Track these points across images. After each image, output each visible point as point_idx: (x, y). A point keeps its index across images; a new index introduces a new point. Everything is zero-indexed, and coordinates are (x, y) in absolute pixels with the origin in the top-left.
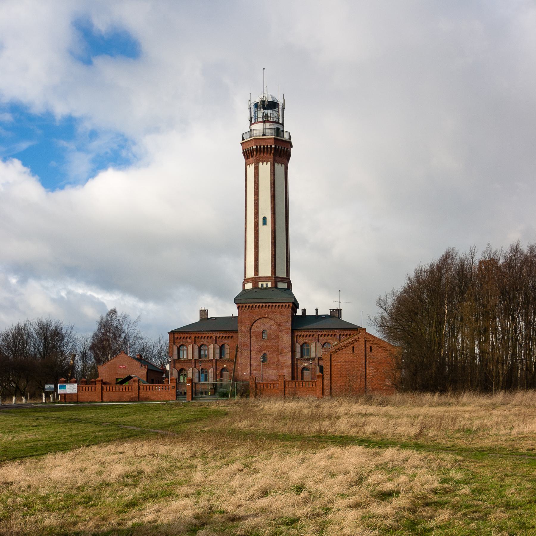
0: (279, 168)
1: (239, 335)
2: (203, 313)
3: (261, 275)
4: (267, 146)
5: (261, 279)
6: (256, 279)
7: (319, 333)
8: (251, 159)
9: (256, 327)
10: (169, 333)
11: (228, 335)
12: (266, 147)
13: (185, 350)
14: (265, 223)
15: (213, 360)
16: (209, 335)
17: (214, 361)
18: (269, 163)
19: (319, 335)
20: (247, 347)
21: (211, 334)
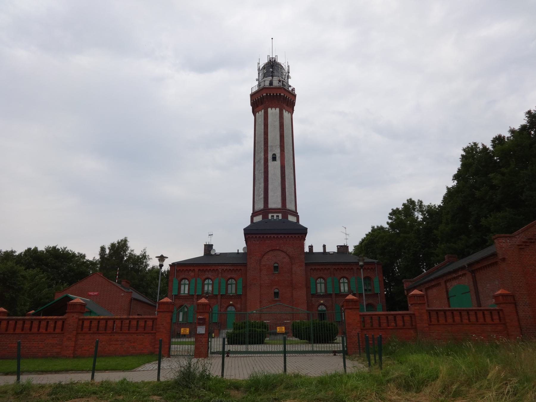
0: (286, 114)
2: (208, 248)
3: (270, 206)
4: (277, 94)
5: (270, 211)
6: (265, 211)
7: (334, 267)
8: (260, 107)
9: (267, 260)
12: (275, 94)
13: (187, 284)
14: (274, 159)
15: (218, 296)
17: (219, 297)
18: (278, 110)
19: (334, 268)
20: (256, 281)
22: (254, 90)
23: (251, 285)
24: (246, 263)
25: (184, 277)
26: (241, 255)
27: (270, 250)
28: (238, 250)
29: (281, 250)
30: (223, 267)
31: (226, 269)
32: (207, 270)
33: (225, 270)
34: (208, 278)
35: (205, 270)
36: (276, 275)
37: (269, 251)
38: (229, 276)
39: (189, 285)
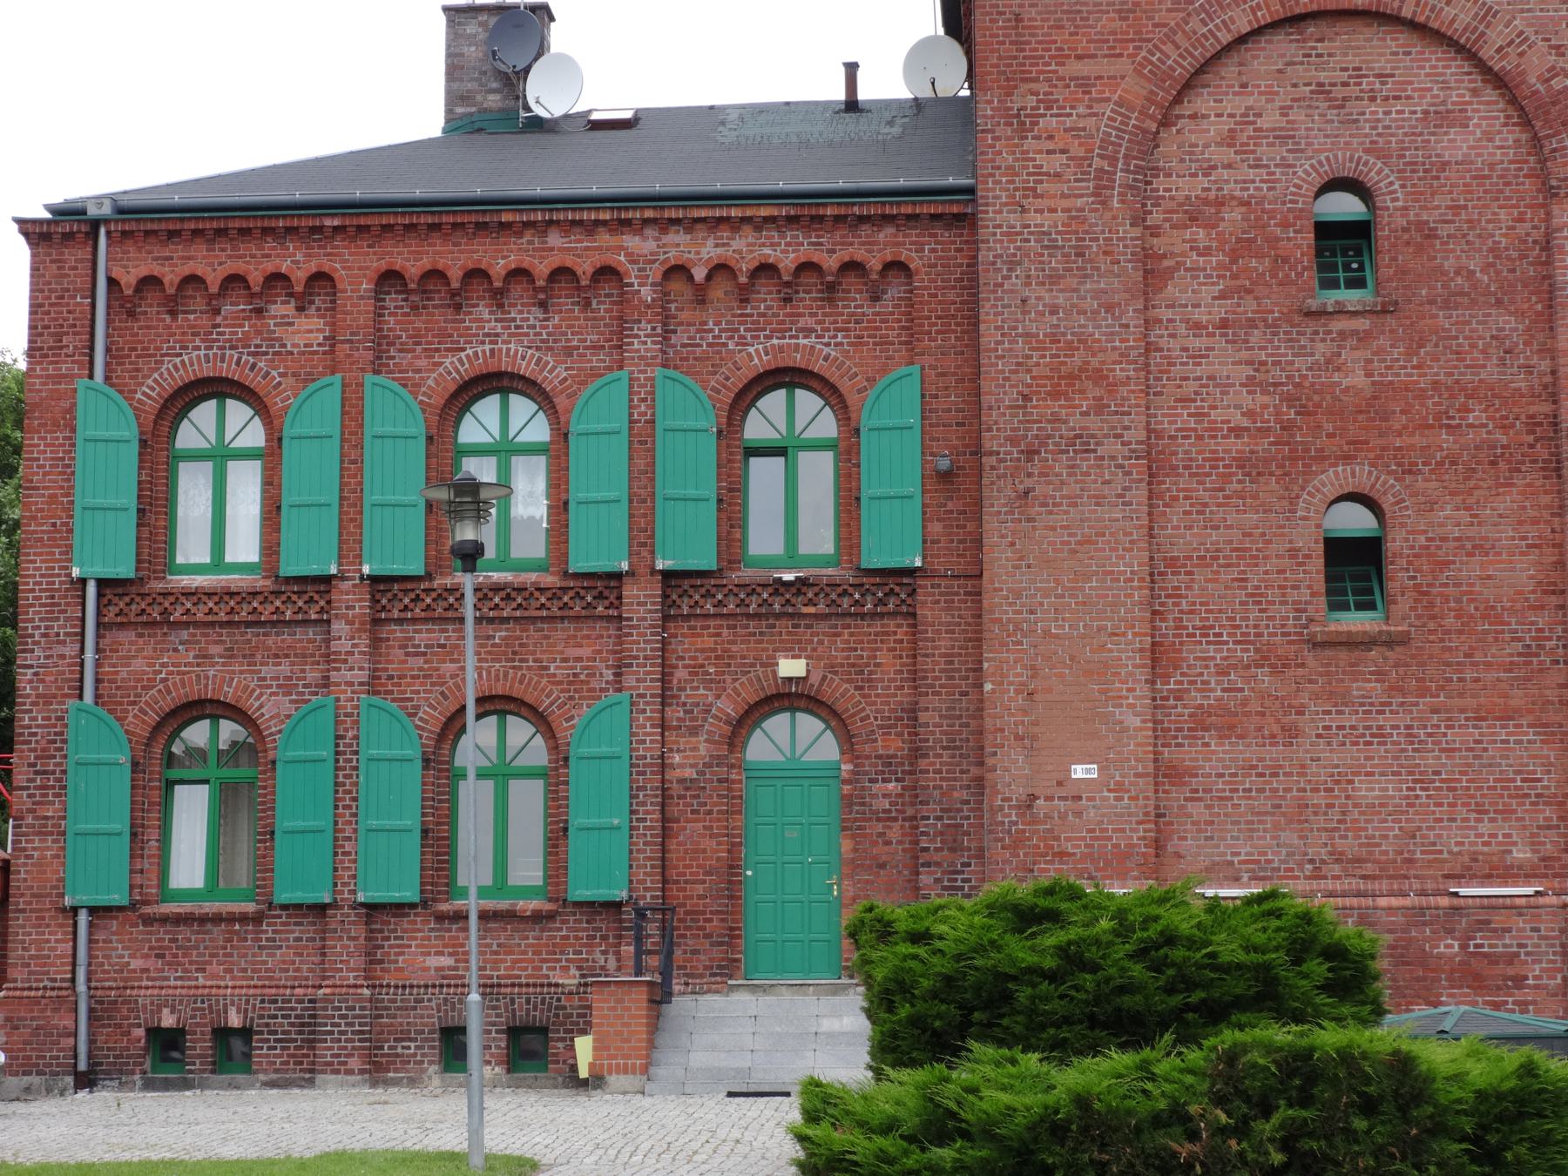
1: (993, 246)
9: (1230, 139)
10: (21, 222)
11: (829, 251)
15: (630, 591)
16: (585, 255)
17: (641, 600)
21: (604, 238)
23: (1031, 453)
24: (970, 191)
25: (207, 371)
26: (890, 123)
27: (1264, 17)
28: (852, 69)
29: (1414, 26)
30: (678, 246)
31: (721, 269)
32: (476, 274)
33: (699, 274)
34: (499, 375)
35: (455, 275)
36: (1339, 325)
37: (1258, 32)
38: (758, 355)
39: (271, 457)
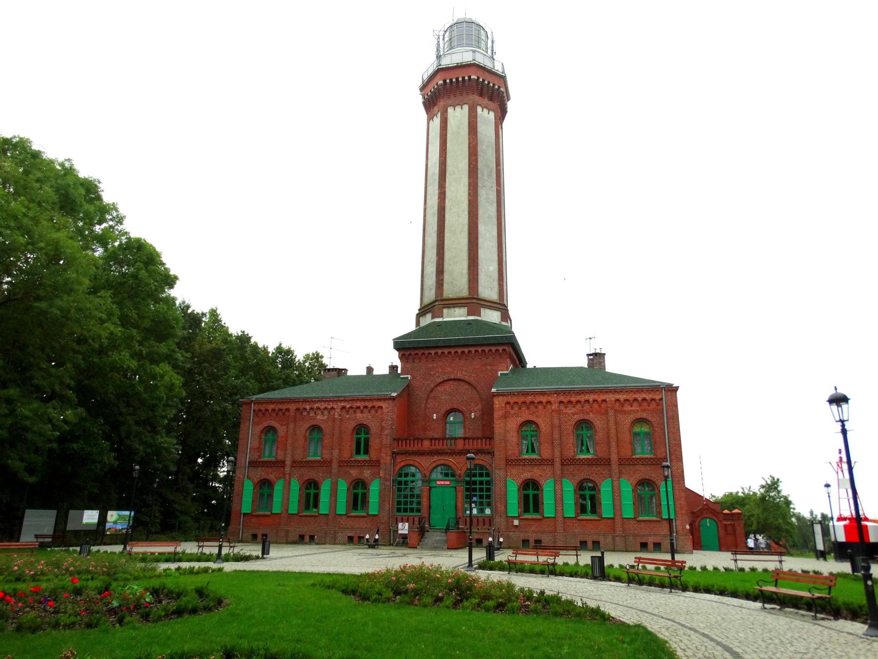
0: (486, 116)
18: (466, 108)
22: (426, 77)
